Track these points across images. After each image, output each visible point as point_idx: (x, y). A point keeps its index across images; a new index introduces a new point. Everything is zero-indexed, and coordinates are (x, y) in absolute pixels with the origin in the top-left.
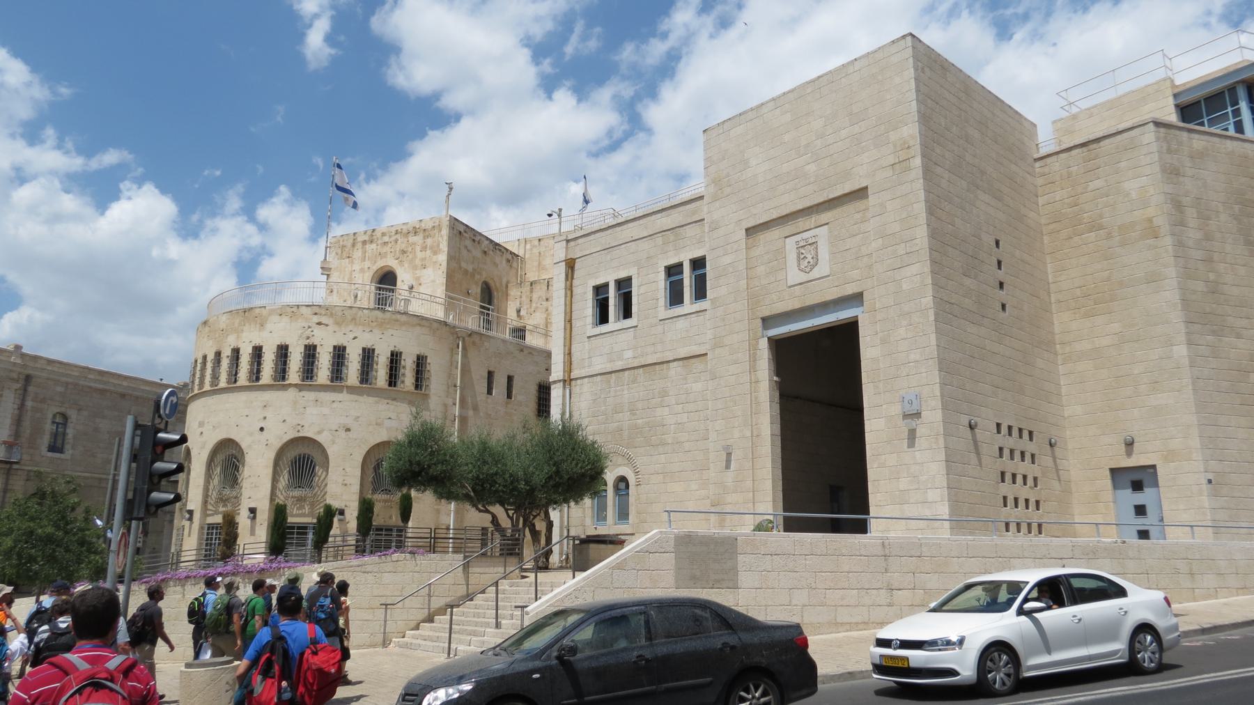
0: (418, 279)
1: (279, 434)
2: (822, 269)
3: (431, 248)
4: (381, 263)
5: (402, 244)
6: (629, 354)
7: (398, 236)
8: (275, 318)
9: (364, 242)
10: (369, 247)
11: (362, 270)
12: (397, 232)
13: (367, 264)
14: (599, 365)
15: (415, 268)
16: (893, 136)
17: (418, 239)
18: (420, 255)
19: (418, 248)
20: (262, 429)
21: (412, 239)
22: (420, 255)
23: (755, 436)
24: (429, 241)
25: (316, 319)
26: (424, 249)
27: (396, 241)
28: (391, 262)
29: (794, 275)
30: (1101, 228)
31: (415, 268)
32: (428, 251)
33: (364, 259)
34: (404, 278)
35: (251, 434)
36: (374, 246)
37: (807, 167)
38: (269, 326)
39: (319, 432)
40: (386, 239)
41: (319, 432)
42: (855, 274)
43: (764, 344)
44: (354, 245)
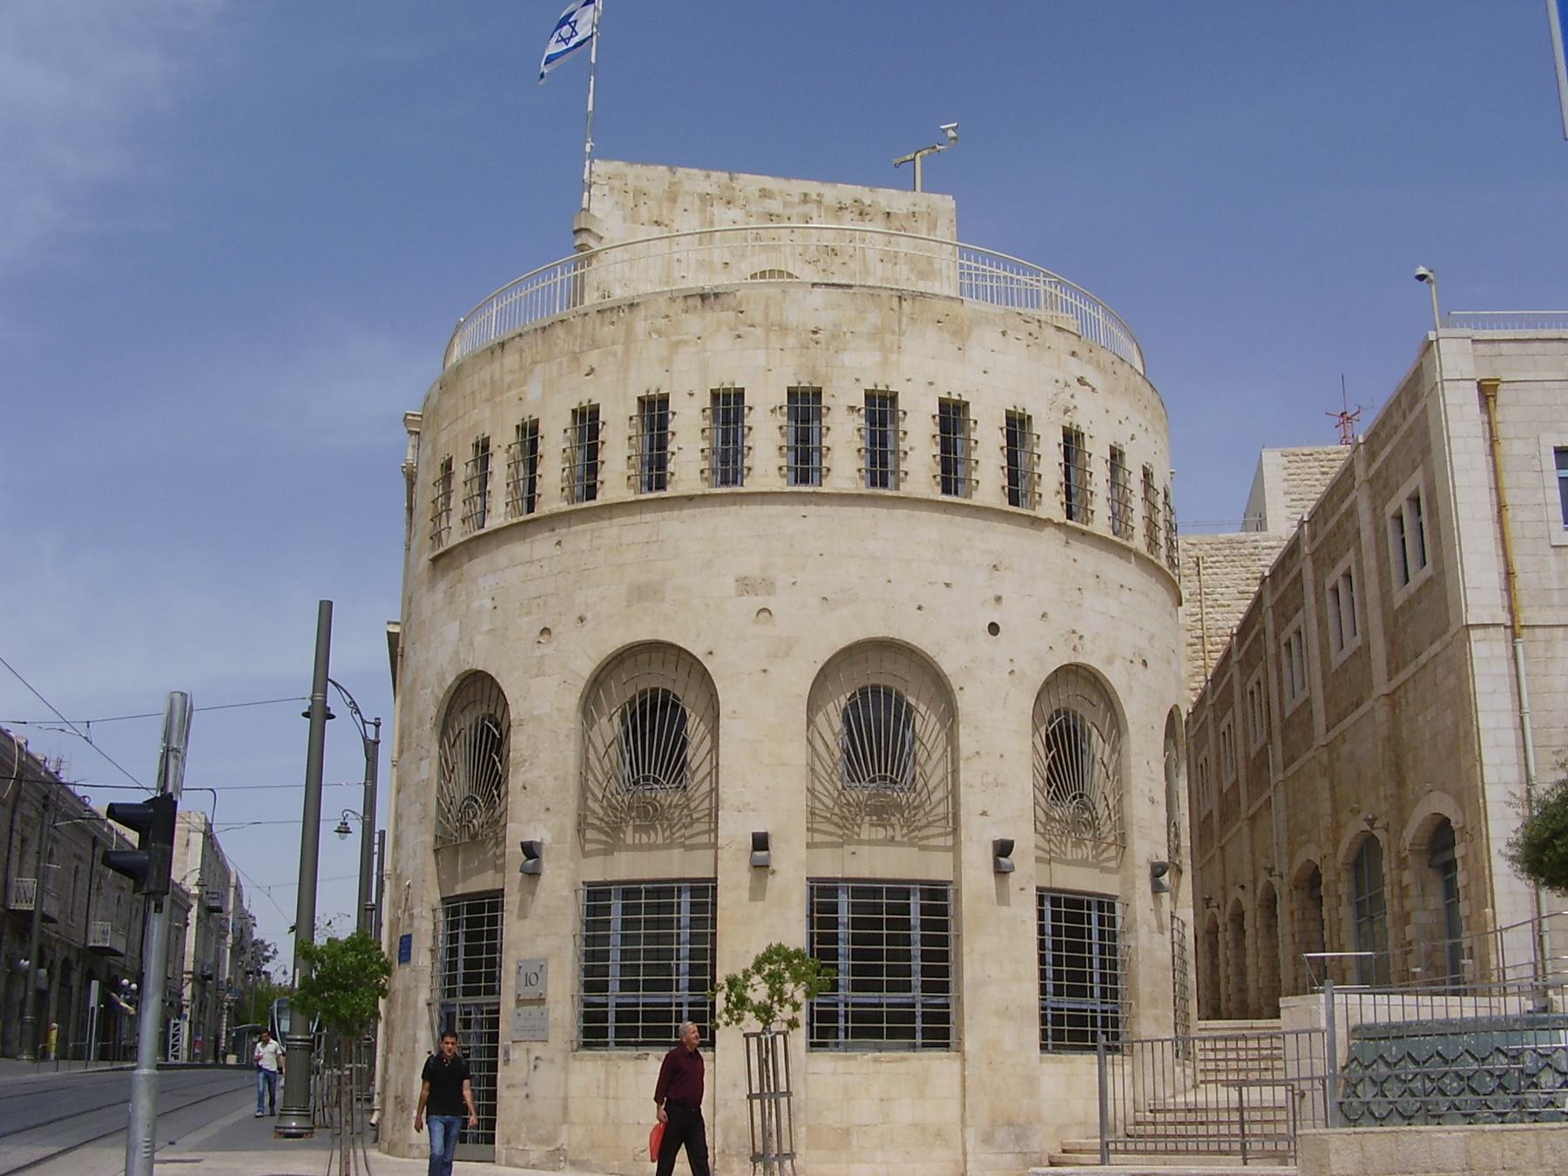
1: (1034, 655)
3: (912, 260)
7: (811, 209)
9: (706, 199)
10: (724, 216)
20: (994, 628)
24: (904, 246)
25: (1076, 368)
36: (735, 213)
39: (1109, 660)
41: (1109, 660)
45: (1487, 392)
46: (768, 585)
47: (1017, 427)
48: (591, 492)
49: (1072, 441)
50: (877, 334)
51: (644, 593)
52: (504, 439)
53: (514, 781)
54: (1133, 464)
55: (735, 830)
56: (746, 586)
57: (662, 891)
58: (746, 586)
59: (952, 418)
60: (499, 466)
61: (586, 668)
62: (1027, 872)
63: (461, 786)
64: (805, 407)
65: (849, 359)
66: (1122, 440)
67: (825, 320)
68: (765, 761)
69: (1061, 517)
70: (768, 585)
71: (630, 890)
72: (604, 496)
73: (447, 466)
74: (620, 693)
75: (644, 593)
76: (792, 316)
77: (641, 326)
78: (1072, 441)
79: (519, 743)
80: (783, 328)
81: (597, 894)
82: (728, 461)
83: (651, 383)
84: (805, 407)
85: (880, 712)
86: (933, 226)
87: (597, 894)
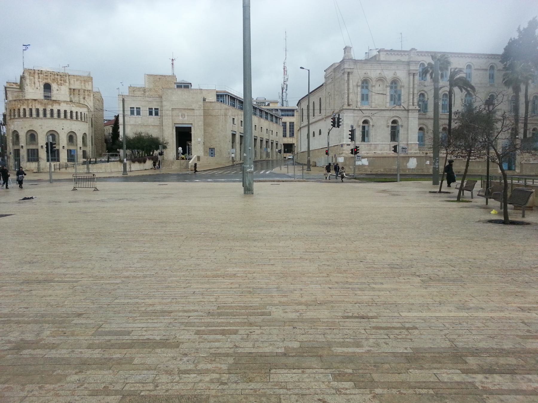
1: (67, 130)
4: (45, 81)
5: (52, 77)
6: (140, 122)
13: (40, 80)
14: (132, 123)
15: (58, 85)
17: (59, 77)
18: (60, 82)
22: (60, 82)
23: (173, 141)
24: (63, 79)
26: (61, 80)
28: (49, 81)
32: (62, 82)
33: (39, 78)
34: (54, 86)
44: (34, 73)
47: (65, 111)
49: (71, 112)
52: (16, 110)
53: (20, 140)
55: (40, 145)
57: (34, 150)
58: (40, 126)
59: (59, 111)
61: (26, 132)
62: (66, 148)
63: (15, 140)
64: (45, 110)
71: (31, 149)
74: (29, 134)
78: (71, 112)
79: (20, 137)
82: (38, 115)
83: (30, 107)
84: (45, 110)
87: (28, 150)
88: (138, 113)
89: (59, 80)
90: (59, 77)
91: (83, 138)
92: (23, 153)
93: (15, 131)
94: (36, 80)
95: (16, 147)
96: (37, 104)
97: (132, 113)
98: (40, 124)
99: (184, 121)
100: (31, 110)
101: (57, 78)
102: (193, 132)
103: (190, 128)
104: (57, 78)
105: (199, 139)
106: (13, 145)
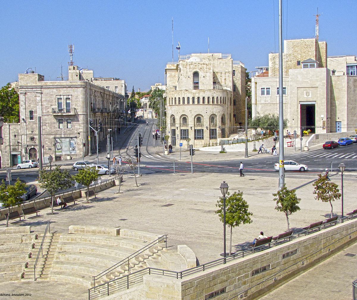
0: (206, 75)
1: (210, 114)
2: (310, 96)
3: (208, 68)
5: (200, 66)
6: (269, 101)
7: (199, 64)
8: (207, 92)
9: (190, 65)
10: (191, 66)
11: (190, 71)
12: (199, 63)
13: (191, 70)
14: (263, 102)
16: (322, 81)
17: (205, 66)
19: (205, 68)
21: (203, 65)
22: (205, 70)
24: (208, 67)
27: (199, 65)
28: (197, 70)
29: (305, 96)
30: (338, 89)
31: (204, 72)
32: (208, 69)
33: (190, 68)
34: (201, 74)
35: (205, 113)
36: (192, 66)
37: (309, 82)
38: (206, 93)
39: (216, 113)
40: (196, 65)
42: (315, 98)
43: (299, 105)
45: (256, 83)
46: (191, 111)
47: (208, 98)
48: (180, 103)
49: (213, 98)
50: (198, 93)
51: (184, 111)
52: (174, 98)
54: (219, 98)
56: (190, 111)
57: (185, 130)
58: (190, 111)
60: (174, 100)
63: (172, 122)
64: (193, 98)
65: (196, 95)
66: (218, 96)
67: (195, 92)
68: (191, 122)
69: (212, 104)
70: (191, 111)
72: (181, 104)
73: (170, 98)
75: (184, 111)
76: (192, 92)
77: (182, 92)
80: (192, 93)
81: (182, 130)
83: (183, 96)
84: (193, 98)
85: (199, 119)
86: (210, 65)
88: (268, 93)
89: (205, 68)
90: (205, 66)
91: (222, 118)
92: (178, 132)
93: (172, 115)
94: (188, 70)
95: (173, 128)
96: (188, 94)
97: (263, 93)
98: (190, 109)
99: (308, 99)
100: (184, 98)
101: (204, 67)
102: (316, 109)
103: (315, 104)
104: (204, 67)
105: (322, 116)
106: (171, 126)
